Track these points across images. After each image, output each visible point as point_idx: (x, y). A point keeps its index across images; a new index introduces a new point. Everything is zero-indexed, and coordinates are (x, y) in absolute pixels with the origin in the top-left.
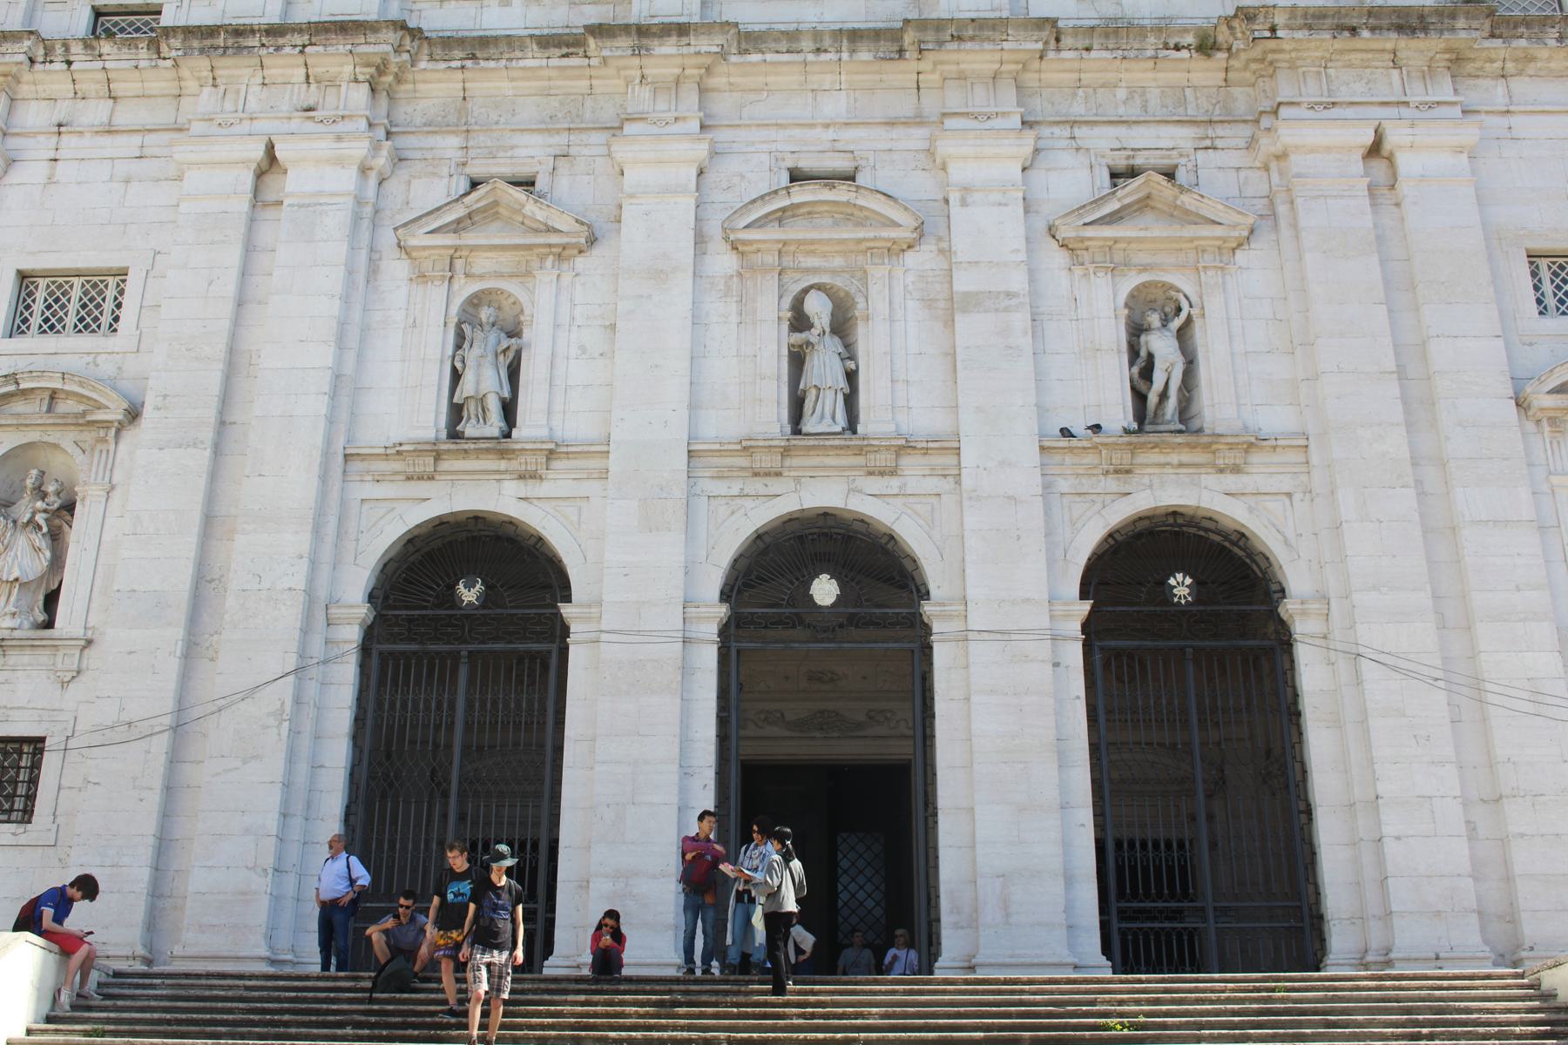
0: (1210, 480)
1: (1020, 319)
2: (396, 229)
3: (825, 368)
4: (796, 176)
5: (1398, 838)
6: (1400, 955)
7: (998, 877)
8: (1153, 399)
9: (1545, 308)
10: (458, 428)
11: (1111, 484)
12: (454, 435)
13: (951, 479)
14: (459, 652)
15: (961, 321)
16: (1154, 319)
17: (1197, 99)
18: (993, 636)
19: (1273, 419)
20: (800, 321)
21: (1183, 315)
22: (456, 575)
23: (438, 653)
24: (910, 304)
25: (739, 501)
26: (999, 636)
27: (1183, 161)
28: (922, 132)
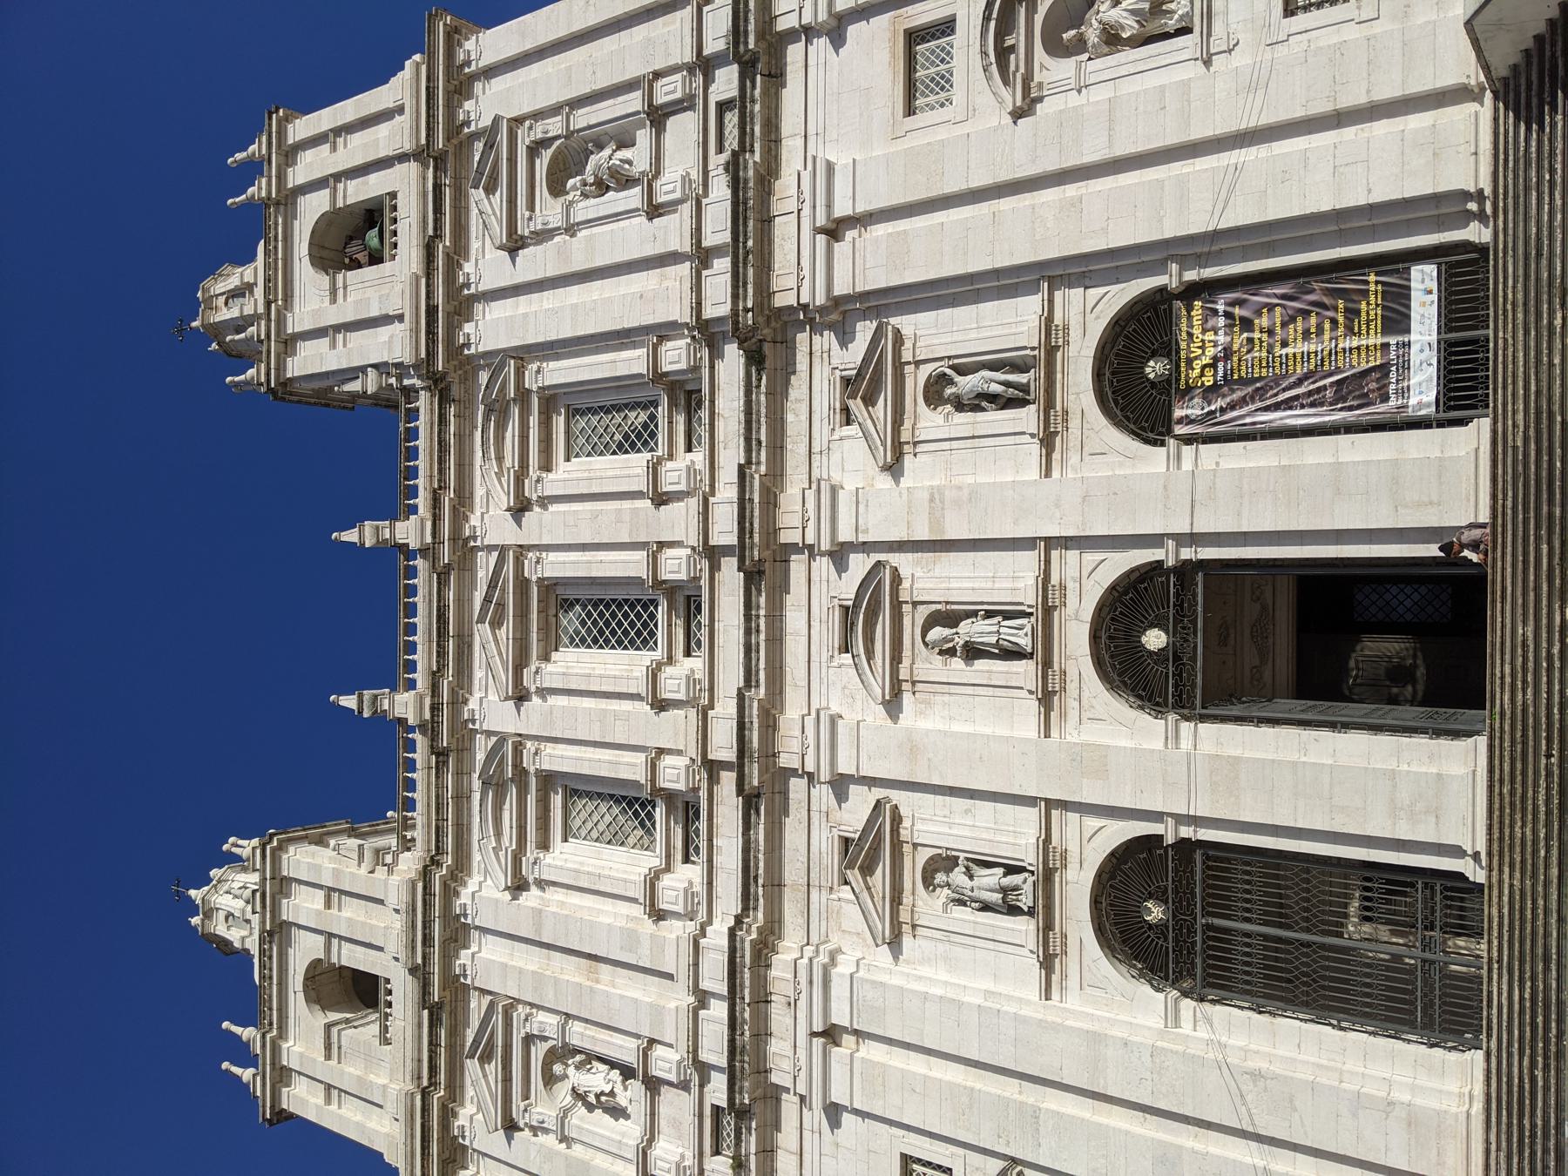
0: (1073, 350)
2: (877, 946)
4: (846, 648)
5: (1369, 191)
7: (1397, 511)
9: (947, 100)
10: (1026, 909)
11: (1074, 423)
12: (1031, 912)
14: (1203, 926)
16: (949, 391)
21: (948, 371)
22: (1141, 922)
23: (1204, 942)
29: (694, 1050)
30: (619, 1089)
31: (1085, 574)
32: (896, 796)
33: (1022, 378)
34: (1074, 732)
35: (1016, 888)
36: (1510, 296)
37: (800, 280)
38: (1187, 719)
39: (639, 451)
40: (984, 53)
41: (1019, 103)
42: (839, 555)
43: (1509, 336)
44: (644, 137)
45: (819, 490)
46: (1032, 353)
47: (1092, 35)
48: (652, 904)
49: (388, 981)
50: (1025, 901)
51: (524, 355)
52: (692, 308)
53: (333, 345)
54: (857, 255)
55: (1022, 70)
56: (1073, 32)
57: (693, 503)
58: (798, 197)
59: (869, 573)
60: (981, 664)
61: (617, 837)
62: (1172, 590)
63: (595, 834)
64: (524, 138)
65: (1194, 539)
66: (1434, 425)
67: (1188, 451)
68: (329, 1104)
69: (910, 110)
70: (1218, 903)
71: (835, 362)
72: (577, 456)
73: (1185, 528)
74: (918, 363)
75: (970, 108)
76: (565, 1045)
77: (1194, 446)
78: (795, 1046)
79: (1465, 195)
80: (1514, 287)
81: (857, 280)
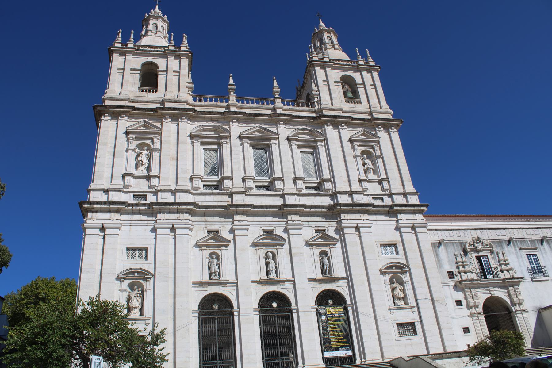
0: (334, 284)
3: (272, 266)
8: (324, 271)
11: (319, 285)
16: (324, 256)
20: (267, 257)
25: (260, 290)
29: (161, 191)
30: (143, 167)
31: (288, 289)
32: (232, 244)
33: (327, 273)
34: (254, 287)
35: (216, 275)
38: (259, 312)
40: (392, 263)
41: (383, 271)
42: (286, 230)
44: (375, 178)
46: (333, 275)
47: (394, 285)
48: (194, 178)
49: (156, 91)
50: (213, 277)
51: (326, 141)
53: (324, 81)
56: (395, 281)
57: (294, 190)
59: (283, 238)
60: (265, 266)
61: (206, 165)
62: (285, 308)
63: (206, 158)
64: (375, 145)
65: (298, 312)
67: (315, 310)
68: (118, 69)
70: (221, 321)
71: (329, 228)
73: (300, 310)
74: (330, 249)
76: (153, 151)
78: (168, 219)
79: (365, 359)
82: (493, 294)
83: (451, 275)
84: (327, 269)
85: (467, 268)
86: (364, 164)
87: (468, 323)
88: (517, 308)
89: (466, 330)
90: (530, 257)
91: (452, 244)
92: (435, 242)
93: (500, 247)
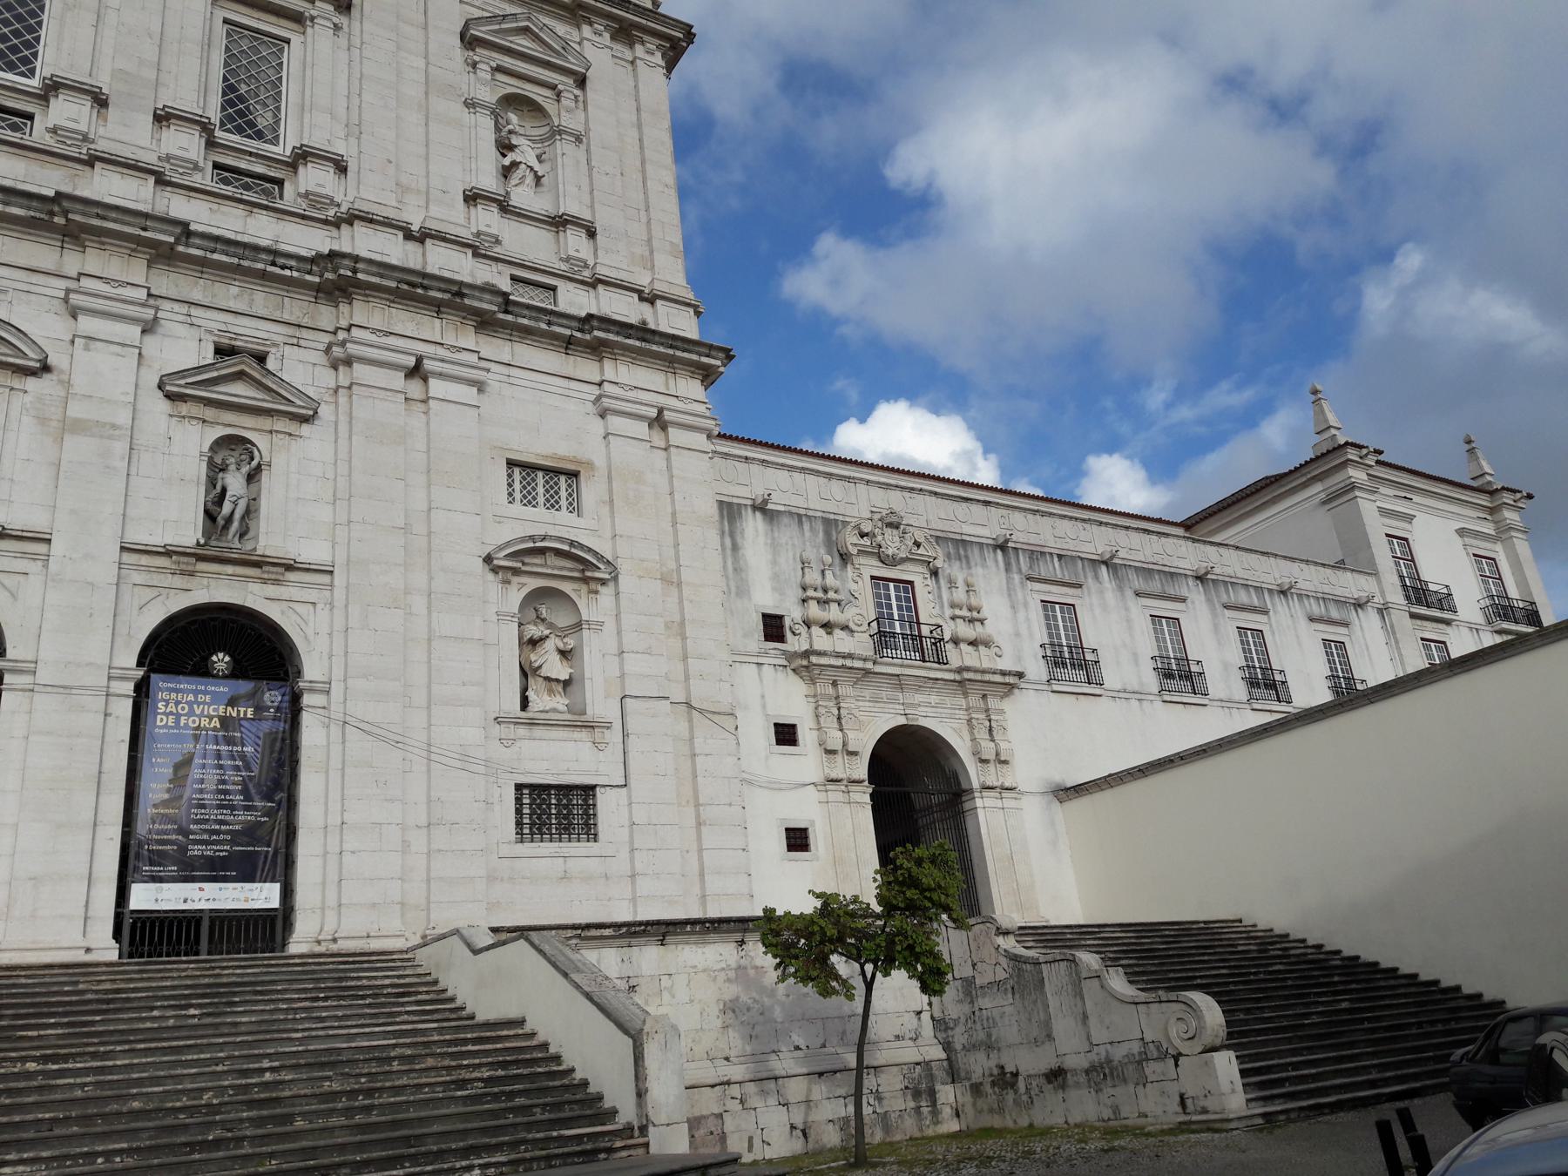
0: (256, 587)
1: (121, 447)
5: (353, 852)
6: (343, 935)
7: (30, 879)
8: (220, 521)
11: (178, 581)
13: (40, 563)
15: (67, 437)
17: (292, 306)
18: (55, 690)
19: (311, 552)
21: (254, 463)
24: (25, 419)
26: (61, 690)
27: (273, 350)
28: (63, 284)
36: (226, 972)
37: (374, 331)
39: (223, 109)
43: (189, 973)
45: (143, 305)
52: (368, 213)
54: (389, 393)
55: (524, 568)
58: (455, 347)
66: (119, 910)
67: (129, 688)
69: (511, 464)
72: (228, 34)
75: (502, 519)
77: (132, 693)
80: (233, 974)
81: (363, 388)
82: (913, 719)
83: (773, 628)
84: (237, 516)
85: (833, 613)
86: (505, 147)
87: (806, 810)
88: (992, 776)
89: (797, 840)
90: (1054, 610)
91: (796, 516)
92: (735, 501)
93: (960, 559)
